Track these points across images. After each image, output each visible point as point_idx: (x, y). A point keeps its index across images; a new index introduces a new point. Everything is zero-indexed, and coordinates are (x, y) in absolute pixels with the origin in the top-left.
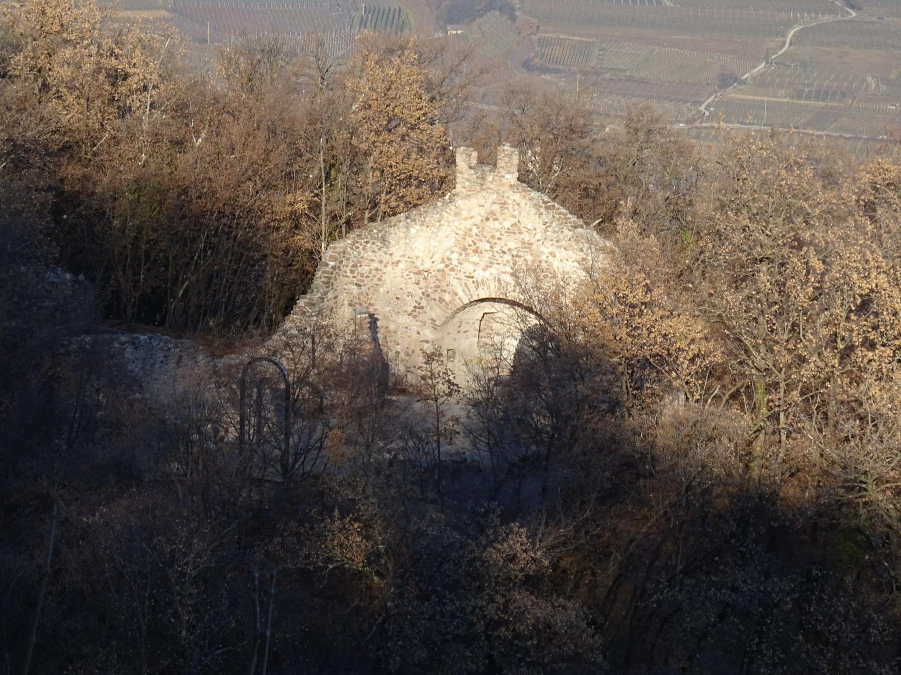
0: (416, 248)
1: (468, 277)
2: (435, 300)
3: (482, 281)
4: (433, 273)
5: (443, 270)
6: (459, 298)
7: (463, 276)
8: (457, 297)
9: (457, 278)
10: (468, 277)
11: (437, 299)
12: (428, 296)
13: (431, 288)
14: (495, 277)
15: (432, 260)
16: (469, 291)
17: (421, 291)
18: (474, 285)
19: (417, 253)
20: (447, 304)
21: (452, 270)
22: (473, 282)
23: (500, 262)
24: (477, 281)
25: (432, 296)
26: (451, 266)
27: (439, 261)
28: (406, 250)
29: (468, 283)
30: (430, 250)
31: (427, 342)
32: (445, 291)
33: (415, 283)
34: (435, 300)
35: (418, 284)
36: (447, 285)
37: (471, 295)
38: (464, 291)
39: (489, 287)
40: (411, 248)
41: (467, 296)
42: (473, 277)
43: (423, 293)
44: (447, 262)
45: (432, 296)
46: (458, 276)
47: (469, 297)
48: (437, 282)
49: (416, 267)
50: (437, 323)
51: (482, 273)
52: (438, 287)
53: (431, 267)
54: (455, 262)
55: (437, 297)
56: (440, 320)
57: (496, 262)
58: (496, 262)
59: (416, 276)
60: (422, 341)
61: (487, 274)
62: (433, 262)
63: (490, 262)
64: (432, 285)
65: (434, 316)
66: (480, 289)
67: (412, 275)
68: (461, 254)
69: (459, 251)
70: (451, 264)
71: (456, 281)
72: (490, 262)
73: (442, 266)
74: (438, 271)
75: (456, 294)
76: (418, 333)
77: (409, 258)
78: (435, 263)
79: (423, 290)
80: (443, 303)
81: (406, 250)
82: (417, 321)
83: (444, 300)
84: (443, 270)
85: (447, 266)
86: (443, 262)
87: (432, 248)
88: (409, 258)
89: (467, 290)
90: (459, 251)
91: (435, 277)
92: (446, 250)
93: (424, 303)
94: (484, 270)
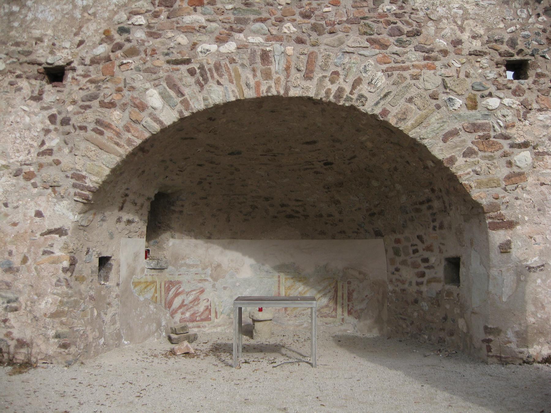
0: (35, 19)
1: (177, 62)
2: (83, 128)
3: (218, 67)
4: (80, 69)
5: (108, 59)
6: (150, 115)
7: (161, 61)
8: (144, 114)
9: (147, 71)
10: (177, 62)
11: (90, 127)
12: (66, 122)
13: (74, 102)
14: (253, 52)
15: (78, 39)
16: (180, 93)
17: (47, 113)
18: (191, 80)
19: (37, 33)
20: (118, 134)
21: (132, 52)
22: (192, 72)
23: (265, 15)
24: (202, 68)
25: (76, 120)
26: (127, 46)
27: (97, 39)
28: (12, 28)
29: (176, 76)
30: (73, 18)
31: (60, 232)
32: (112, 105)
33: (33, 98)
34: (83, 128)
35: (38, 98)
36: (119, 90)
37: (185, 103)
38: (164, 96)
39: (238, 76)
40: (23, 21)
41: (173, 107)
42: (187, 62)
43: (52, 118)
44: (118, 38)
45: (76, 120)
46: (148, 65)
47: (180, 107)
48: (92, 87)
49: (33, 63)
50: (88, 183)
51: (213, 48)
52: (93, 97)
53: (74, 55)
54: (139, 34)
55: (91, 116)
56: (97, 174)
57: (252, 17)
58: (252, 17)
59: (33, 82)
60: (50, 232)
61: (230, 47)
62: (81, 43)
63: (238, 21)
64: (78, 95)
65: (80, 164)
66: (212, 83)
67: (23, 83)
68: (156, 15)
69: (150, 7)
70: (128, 40)
71: (140, 76)
72: (238, 21)
73: (102, 50)
74: (94, 61)
75: (142, 107)
76: (39, 214)
77: (17, 44)
78: (88, 43)
79: (54, 111)
80: (108, 133)
81: (12, 28)
82: (35, 186)
83: (108, 126)
84: (108, 59)
85: (119, 46)
86: (107, 37)
87: (78, 14)
88: (17, 44)
89: (172, 93)
90: (150, 7)
91: (85, 76)
92: (116, 13)
93: (53, 142)
94: (220, 40)
